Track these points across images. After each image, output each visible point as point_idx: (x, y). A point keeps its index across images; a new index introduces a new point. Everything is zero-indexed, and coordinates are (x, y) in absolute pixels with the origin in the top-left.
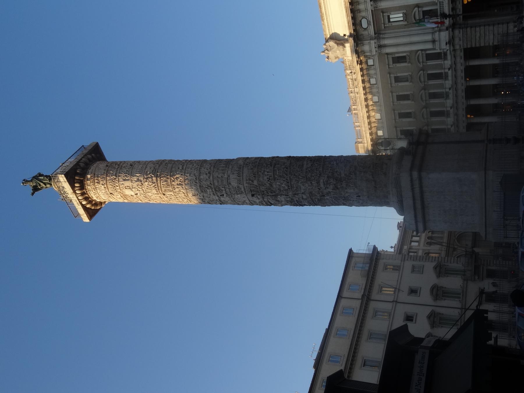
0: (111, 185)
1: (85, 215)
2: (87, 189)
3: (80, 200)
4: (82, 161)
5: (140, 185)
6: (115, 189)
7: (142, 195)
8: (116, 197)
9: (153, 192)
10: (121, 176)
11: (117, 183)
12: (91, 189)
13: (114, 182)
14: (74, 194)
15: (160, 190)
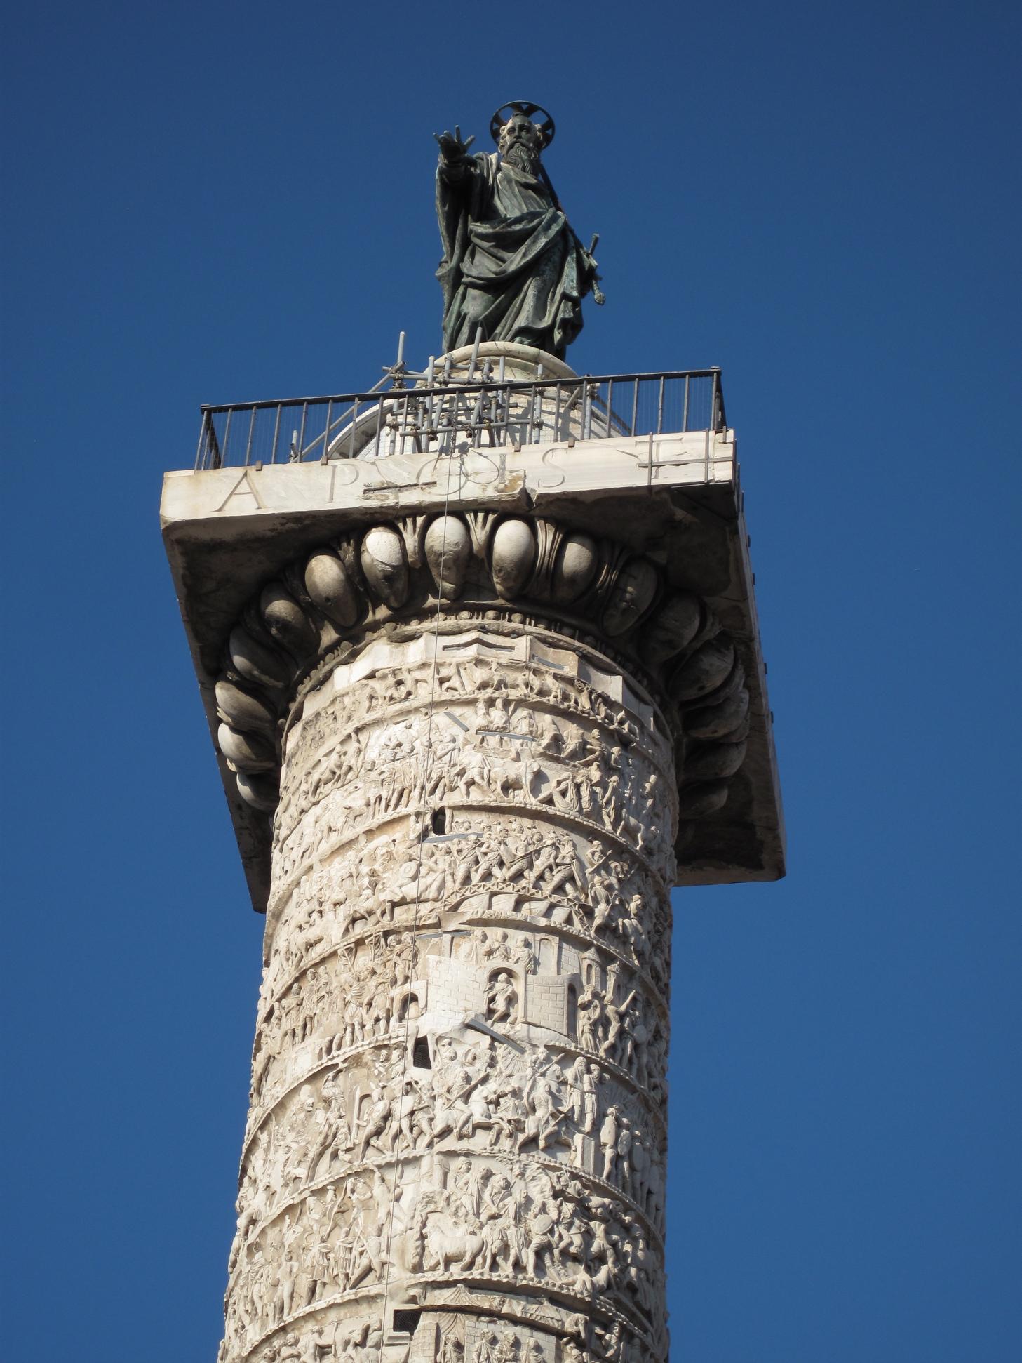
0: (538, 852)
1: (244, 507)
2: (508, 625)
3: (420, 520)
4: (740, 678)
5: (518, 1126)
6: (488, 876)
7: (408, 1103)
8: (401, 848)
9: (445, 1220)
10: (604, 972)
11: (548, 913)
12: (505, 657)
13: (559, 889)
14: (505, 496)
15: (468, 1299)
